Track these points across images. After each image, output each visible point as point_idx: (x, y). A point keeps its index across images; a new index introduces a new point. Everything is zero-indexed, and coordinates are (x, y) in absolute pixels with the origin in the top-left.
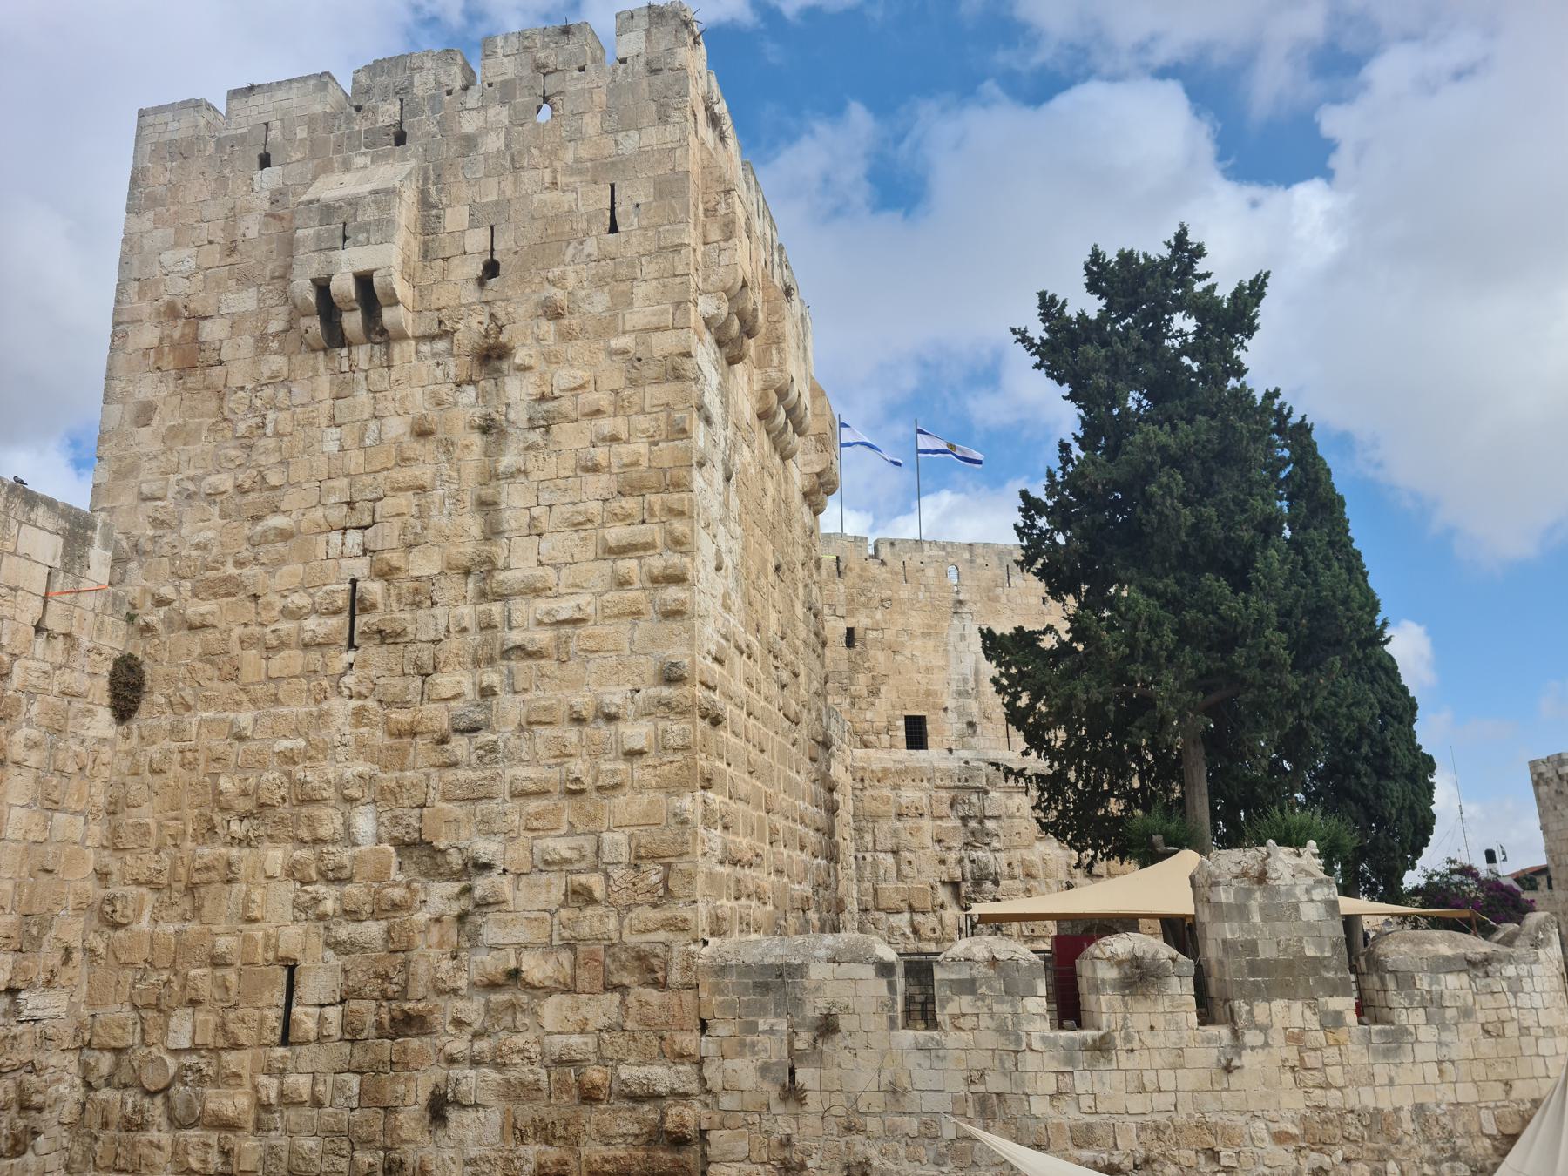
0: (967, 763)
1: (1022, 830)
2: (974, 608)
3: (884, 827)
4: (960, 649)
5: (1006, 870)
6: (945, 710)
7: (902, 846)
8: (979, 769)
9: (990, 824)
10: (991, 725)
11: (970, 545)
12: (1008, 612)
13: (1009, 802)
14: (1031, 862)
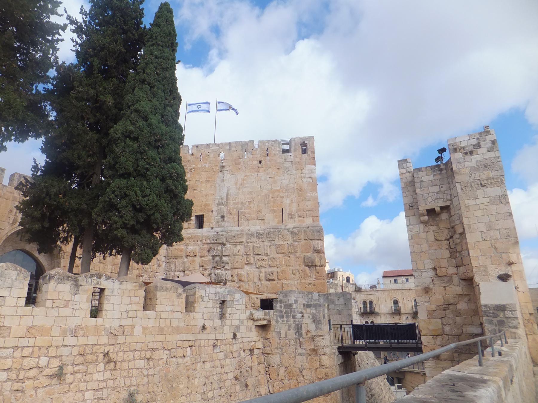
0: (217, 233)
1: (240, 261)
2: (229, 168)
3: (180, 261)
4: (221, 186)
5: (230, 278)
6: (212, 211)
7: (186, 269)
8: (222, 235)
9: (224, 259)
10: (231, 216)
11: (230, 143)
12: (244, 168)
13: (235, 249)
14: (241, 274)
